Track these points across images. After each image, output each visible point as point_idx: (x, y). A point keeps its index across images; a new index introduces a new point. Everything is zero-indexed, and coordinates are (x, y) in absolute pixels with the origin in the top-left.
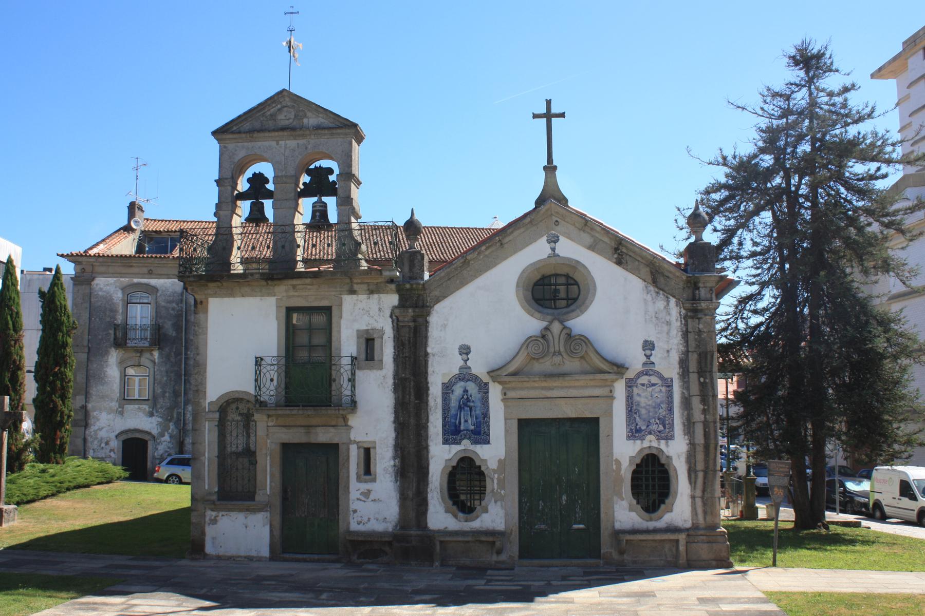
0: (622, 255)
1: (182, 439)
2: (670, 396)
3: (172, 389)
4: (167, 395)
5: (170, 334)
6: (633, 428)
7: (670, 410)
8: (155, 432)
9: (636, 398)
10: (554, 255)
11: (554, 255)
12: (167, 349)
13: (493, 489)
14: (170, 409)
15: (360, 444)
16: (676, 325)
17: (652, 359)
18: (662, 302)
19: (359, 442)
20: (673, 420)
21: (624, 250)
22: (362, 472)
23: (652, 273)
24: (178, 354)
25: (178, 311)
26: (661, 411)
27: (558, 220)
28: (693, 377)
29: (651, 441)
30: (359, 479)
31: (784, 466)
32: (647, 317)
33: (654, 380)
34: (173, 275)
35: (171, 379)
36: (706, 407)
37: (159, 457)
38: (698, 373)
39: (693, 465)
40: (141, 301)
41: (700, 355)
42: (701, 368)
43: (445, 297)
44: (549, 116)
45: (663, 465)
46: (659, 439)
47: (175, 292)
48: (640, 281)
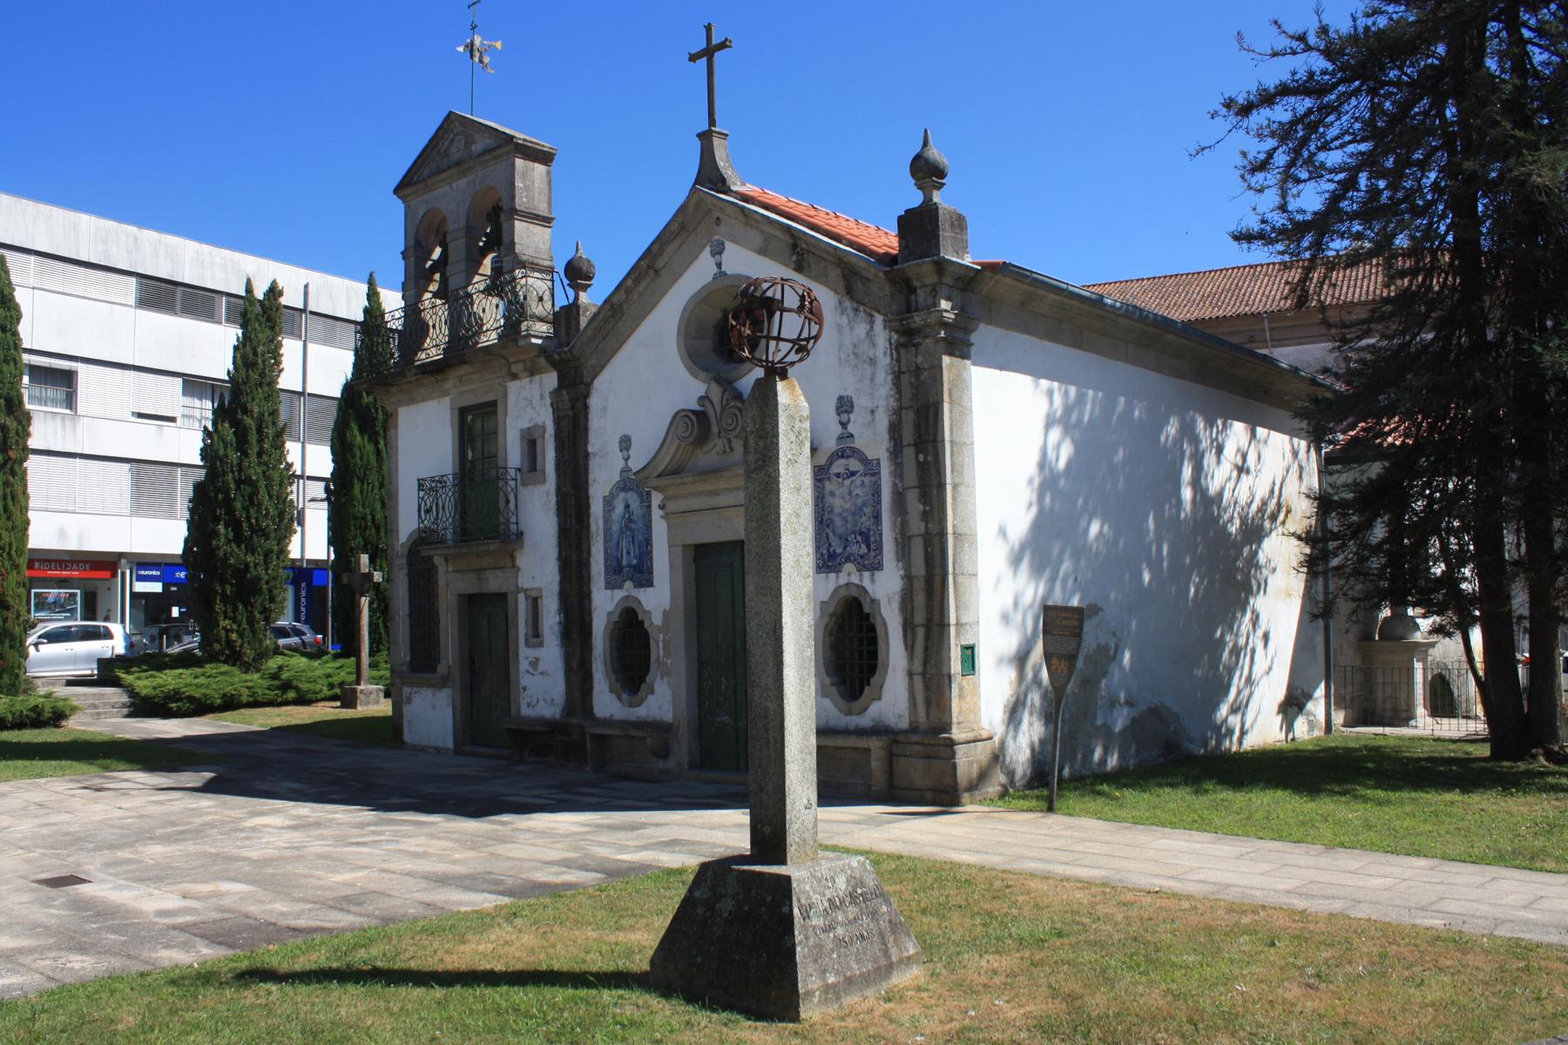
0: (803, 255)
2: (877, 493)
6: (825, 552)
7: (877, 517)
9: (829, 500)
10: (721, 274)
11: (721, 274)
13: (659, 657)
15: (528, 593)
16: (884, 361)
17: (851, 428)
18: (864, 325)
19: (527, 590)
20: (881, 535)
21: (804, 246)
22: (530, 634)
23: (844, 276)
26: (864, 518)
27: (721, 216)
28: (909, 453)
29: (849, 574)
30: (527, 644)
31: (1070, 615)
32: (843, 356)
33: (855, 465)
36: (927, 508)
38: (915, 445)
39: (909, 616)
41: (918, 413)
42: (920, 437)
43: (603, 367)
44: (709, 52)
45: (868, 615)
46: (861, 568)
48: (832, 293)
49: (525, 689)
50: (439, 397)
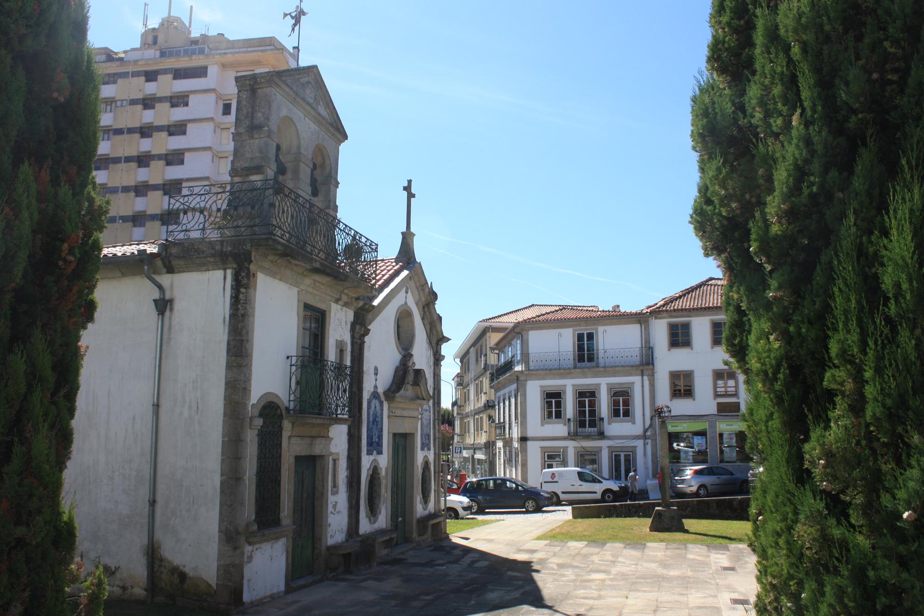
49: (330, 525)
50: (291, 285)
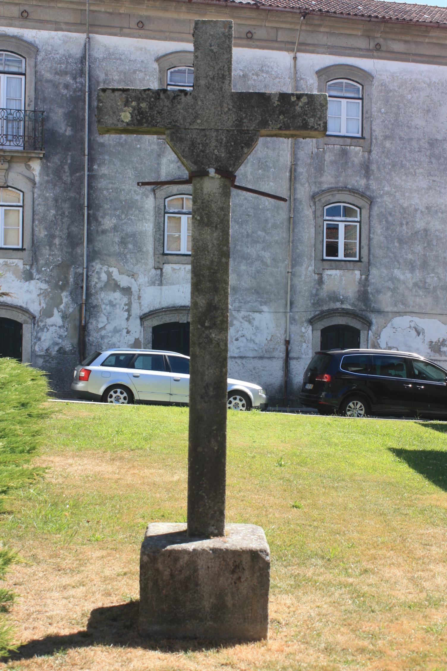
1: (83, 322)
3: (66, 231)
4: (57, 241)
5: (61, 131)
8: (35, 308)
12: (56, 160)
14: (64, 267)
24: (76, 168)
25: (75, 91)
34: (67, 23)
35: (64, 213)
37: (42, 353)
40: (6, 69)
47: (70, 56)
